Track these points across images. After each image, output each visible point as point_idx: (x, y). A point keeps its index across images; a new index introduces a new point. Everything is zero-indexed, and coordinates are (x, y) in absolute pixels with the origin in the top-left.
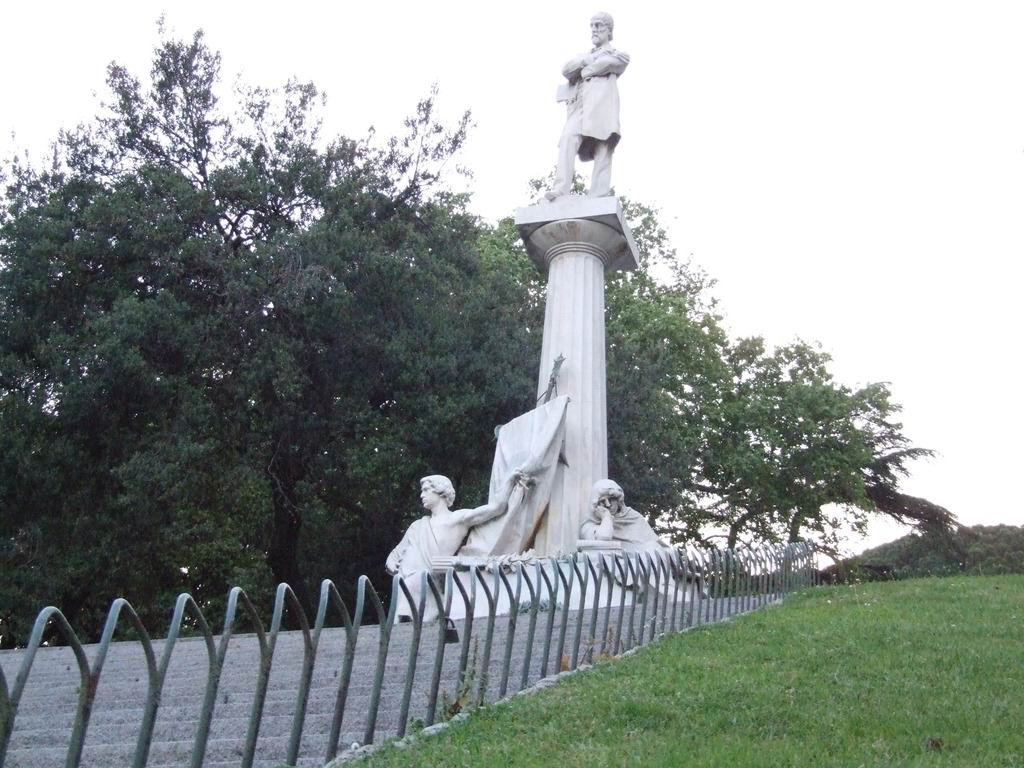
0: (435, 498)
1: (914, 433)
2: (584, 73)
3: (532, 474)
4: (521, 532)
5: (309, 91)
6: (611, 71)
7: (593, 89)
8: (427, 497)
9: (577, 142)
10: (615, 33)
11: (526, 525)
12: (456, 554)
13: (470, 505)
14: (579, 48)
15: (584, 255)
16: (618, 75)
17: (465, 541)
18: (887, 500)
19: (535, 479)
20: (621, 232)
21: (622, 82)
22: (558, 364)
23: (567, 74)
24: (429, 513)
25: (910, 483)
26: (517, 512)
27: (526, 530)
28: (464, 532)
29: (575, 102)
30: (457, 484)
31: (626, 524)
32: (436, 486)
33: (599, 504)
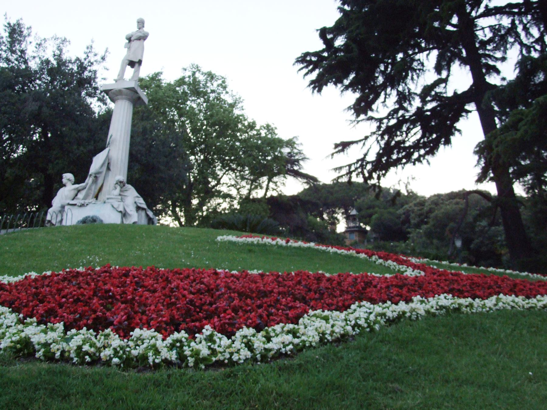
0: (67, 181)
1: (306, 152)
2: (132, 39)
3: (96, 174)
4: (92, 192)
5: (64, 41)
6: (143, 38)
7: (135, 44)
8: (64, 181)
9: (127, 62)
10: (145, 25)
11: (94, 189)
12: (73, 199)
13: (79, 183)
14: (133, 29)
15: (125, 100)
16: (145, 40)
17: (76, 195)
18: (297, 174)
19: (98, 175)
20: (137, 93)
21: (146, 43)
22: (111, 137)
23: (127, 39)
24: (65, 186)
25: (306, 168)
26: (91, 186)
27: (94, 192)
28: (76, 192)
29: (129, 48)
30: (75, 176)
31: (126, 190)
32: (68, 177)
33: (117, 183)
